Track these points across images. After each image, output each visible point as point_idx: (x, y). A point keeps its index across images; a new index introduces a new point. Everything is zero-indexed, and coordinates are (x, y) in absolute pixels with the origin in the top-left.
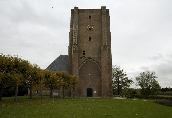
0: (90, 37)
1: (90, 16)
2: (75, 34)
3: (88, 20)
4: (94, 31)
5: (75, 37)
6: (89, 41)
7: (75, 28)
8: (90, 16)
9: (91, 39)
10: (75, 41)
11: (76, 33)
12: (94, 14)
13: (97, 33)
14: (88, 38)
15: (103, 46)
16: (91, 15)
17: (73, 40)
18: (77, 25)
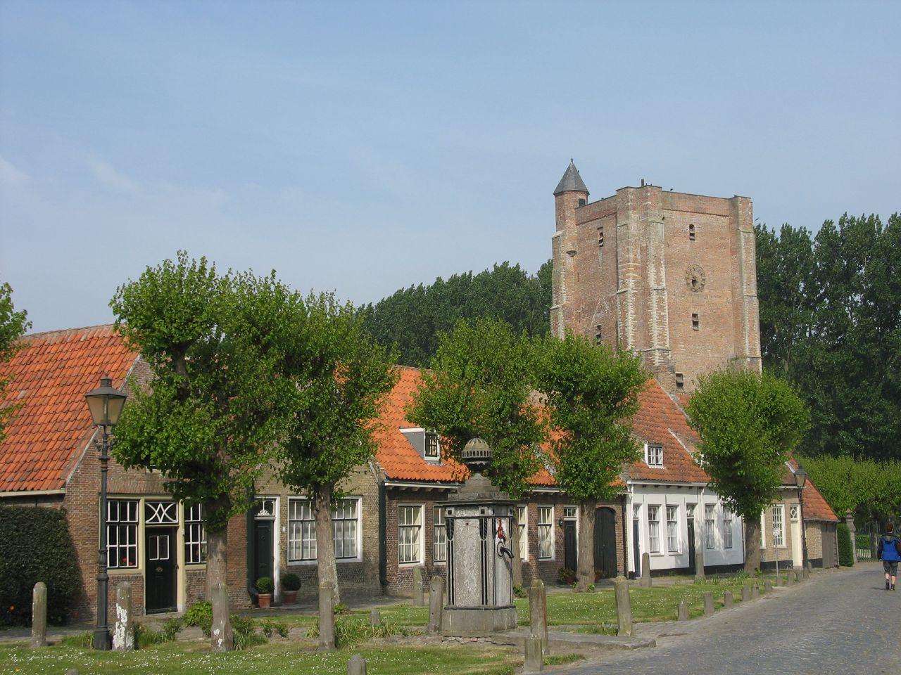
0: (695, 315)
1: (691, 227)
2: (661, 308)
3: (687, 245)
4: (706, 291)
5: (661, 317)
6: (694, 333)
7: (658, 280)
8: (691, 227)
9: (700, 325)
10: (661, 335)
11: (663, 300)
12: (703, 219)
13: (718, 300)
14: (690, 319)
15: (749, 360)
16: (697, 219)
17: (655, 330)
18: (664, 269)
